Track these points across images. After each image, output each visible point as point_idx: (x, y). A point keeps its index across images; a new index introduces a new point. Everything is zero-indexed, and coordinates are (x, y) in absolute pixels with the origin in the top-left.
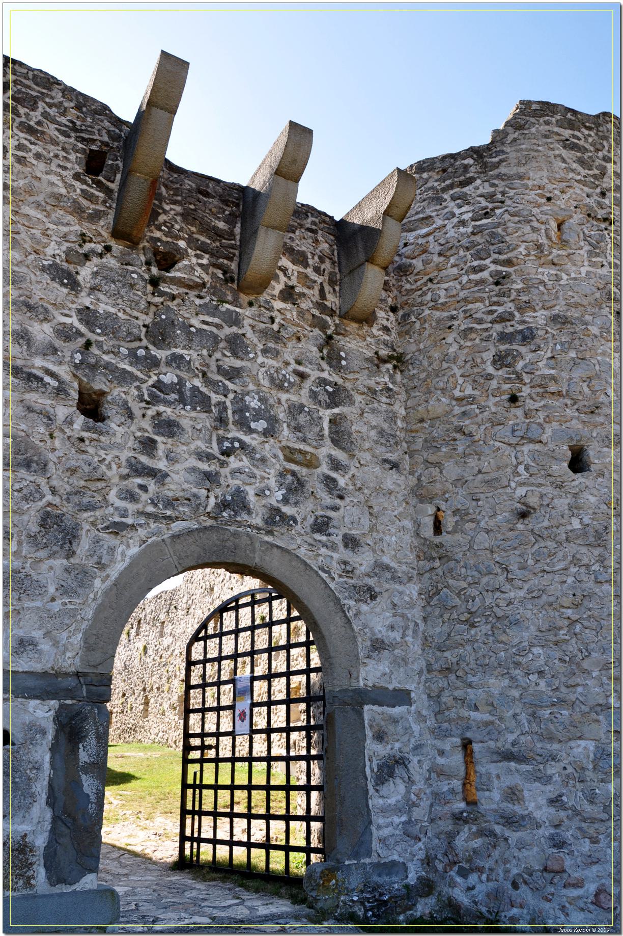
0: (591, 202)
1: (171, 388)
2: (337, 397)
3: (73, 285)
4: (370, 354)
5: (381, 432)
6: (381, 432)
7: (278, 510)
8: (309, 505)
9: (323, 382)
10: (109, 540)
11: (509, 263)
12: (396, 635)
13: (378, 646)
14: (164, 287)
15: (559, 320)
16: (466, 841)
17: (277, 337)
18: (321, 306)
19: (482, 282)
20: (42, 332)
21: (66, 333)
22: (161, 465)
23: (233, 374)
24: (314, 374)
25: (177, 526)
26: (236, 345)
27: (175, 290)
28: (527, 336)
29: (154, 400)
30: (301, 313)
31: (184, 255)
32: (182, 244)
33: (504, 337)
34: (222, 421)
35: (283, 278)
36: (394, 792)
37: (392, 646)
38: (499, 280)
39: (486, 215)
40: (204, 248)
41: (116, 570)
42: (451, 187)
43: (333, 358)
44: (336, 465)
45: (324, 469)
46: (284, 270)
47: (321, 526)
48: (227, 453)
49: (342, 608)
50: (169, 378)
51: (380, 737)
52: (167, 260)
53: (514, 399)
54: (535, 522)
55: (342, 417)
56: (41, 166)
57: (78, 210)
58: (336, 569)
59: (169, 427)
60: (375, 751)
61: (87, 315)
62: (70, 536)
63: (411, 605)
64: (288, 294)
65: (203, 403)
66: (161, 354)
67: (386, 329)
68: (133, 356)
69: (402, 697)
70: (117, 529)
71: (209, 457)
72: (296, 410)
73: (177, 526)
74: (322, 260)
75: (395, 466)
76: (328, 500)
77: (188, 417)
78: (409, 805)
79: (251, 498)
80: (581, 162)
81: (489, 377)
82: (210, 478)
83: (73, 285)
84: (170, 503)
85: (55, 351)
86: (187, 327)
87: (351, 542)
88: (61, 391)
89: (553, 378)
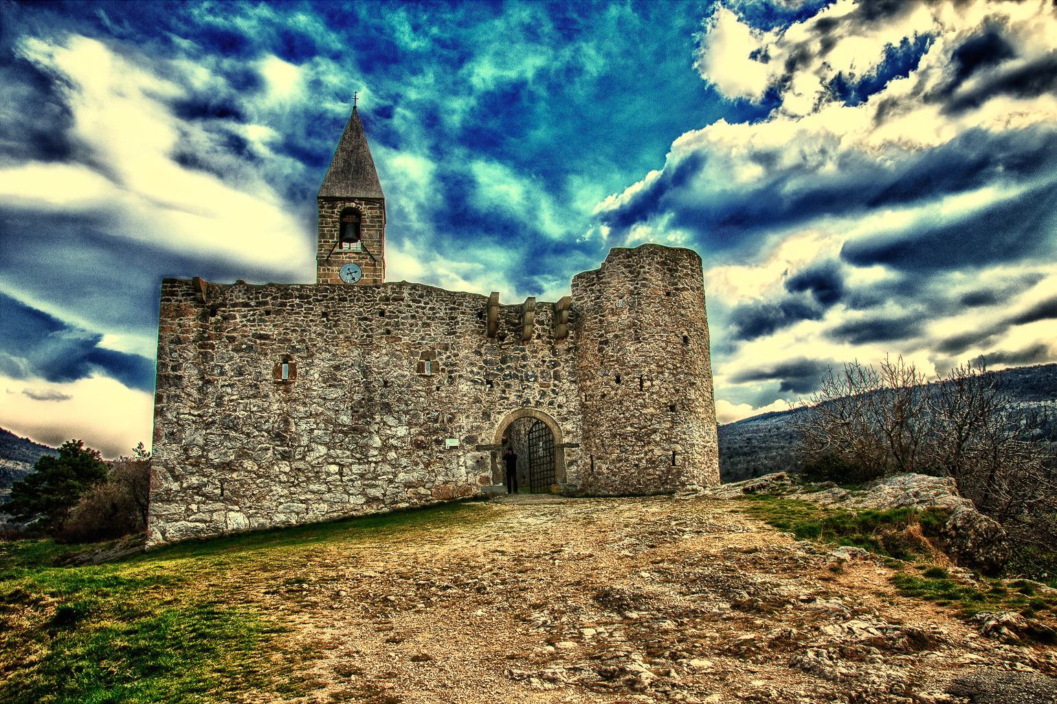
0: (632, 288)
1: (508, 375)
2: (556, 364)
3: (481, 355)
4: (565, 348)
5: (570, 372)
6: (570, 372)
7: (538, 401)
8: (548, 398)
9: (551, 361)
10: (498, 416)
11: (603, 316)
12: (575, 429)
13: (568, 433)
14: (503, 347)
15: (616, 336)
16: (591, 479)
17: (536, 352)
18: (550, 337)
19: (596, 323)
20: (475, 369)
21: (481, 368)
22: (508, 396)
23: (524, 366)
24: (547, 359)
25: (513, 410)
26: (524, 358)
27: (506, 346)
28: (606, 342)
29: (504, 379)
30: (543, 342)
31: (507, 335)
32: (506, 332)
33: (601, 343)
34: (522, 380)
35: (536, 332)
36: (574, 468)
37: (573, 433)
38: (601, 322)
39: (598, 298)
40: (512, 330)
41: (499, 423)
42: (589, 286)
43: (554, 354)
44: (555, 385)
45: (552, 387)
46: (537, 329)
47: (551, 403)
48: (524, 389)
49: (557, 424)
50: (507, 372)
51: (569, 455)
52: (502, 338)
53: (602, 363)
54: (607, 398)
55: (558, 370)
56: (468, 323)
57: (478, 333)
58: (556, 414)
59: (508, 386)
60: (567, 459)
61: (486, 362)
62: (489, 416)
63: (579, 421)
64: (539, 337)
65: (517, 377)
66: (504, 366)
67: (572, 338)
68: (498, 370)
69: (577, 445)
70: (499, 413)
71: (519, 391)
72: (542, 372)
73: (513, 410)
74: (549, 321)
75: (574, 382)
76: (553, 396)
77: (515, 383)
78: (577, 472)
79: (531, 400)
80: (630, 272)
81: (597, 355)
82: (520, 397)
83: (481, 355)
84: (510, 405)
85: (479, 373)
86: (510, 357)
87: (560, 406)
88: (482, 384)
89: (612, 356)
